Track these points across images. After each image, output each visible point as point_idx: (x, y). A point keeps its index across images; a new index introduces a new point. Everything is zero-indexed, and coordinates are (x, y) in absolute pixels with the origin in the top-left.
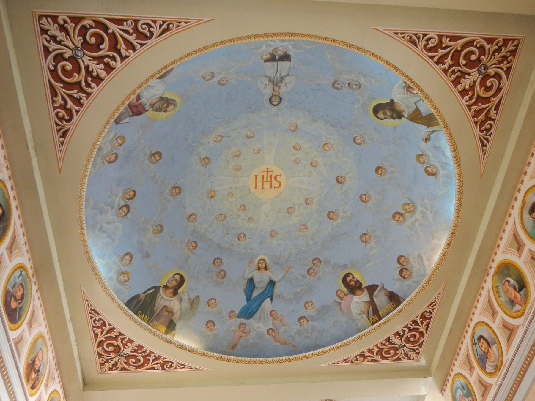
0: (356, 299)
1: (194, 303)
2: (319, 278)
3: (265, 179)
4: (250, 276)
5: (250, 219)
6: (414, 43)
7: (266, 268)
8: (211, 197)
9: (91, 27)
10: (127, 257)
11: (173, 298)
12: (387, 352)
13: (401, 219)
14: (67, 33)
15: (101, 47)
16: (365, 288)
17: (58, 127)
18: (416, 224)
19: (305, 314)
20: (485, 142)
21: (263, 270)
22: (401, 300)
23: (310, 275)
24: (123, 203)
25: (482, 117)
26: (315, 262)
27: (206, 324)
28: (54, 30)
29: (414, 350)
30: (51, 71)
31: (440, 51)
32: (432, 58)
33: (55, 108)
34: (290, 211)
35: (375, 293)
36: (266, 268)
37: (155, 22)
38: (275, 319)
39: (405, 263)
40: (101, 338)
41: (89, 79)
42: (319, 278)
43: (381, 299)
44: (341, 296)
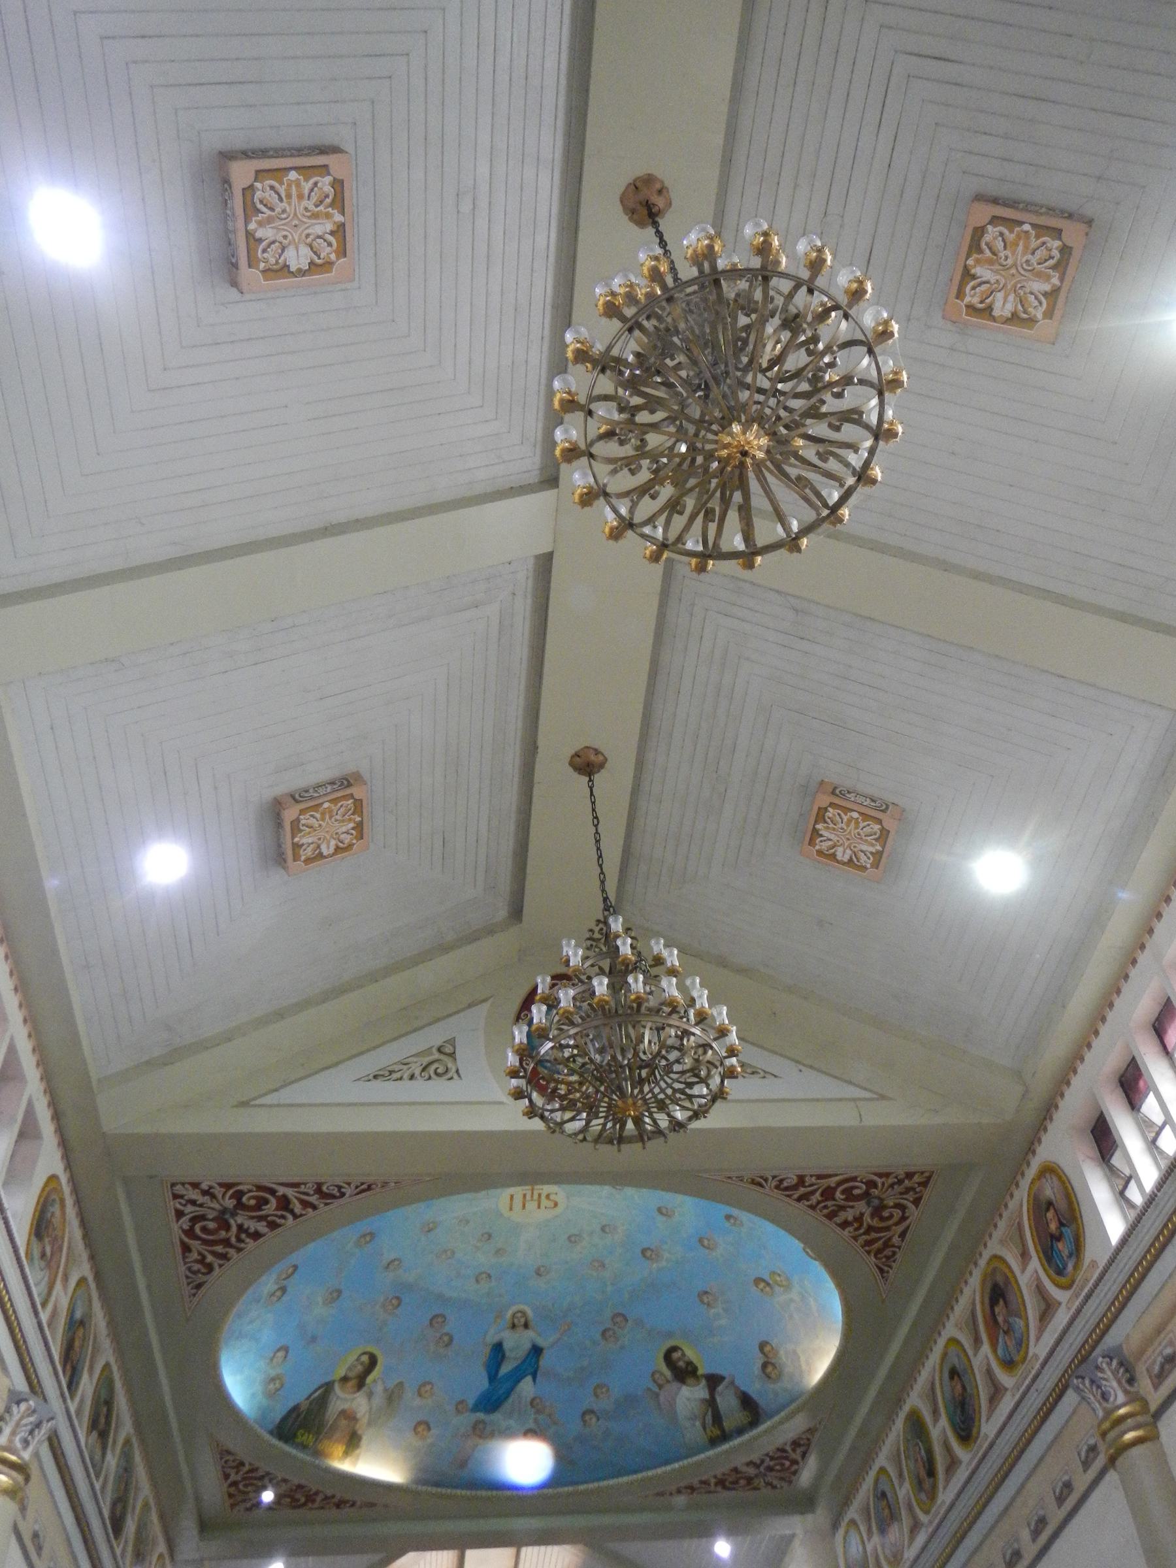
1: (393, 1397)
2: (622, 1347)
3: (528, 1197)
4: (496, 1340)
5: (499, 1252)
7: (526, 1326)
8: (430, 1231)
9: (250, 1191)
10: (281, 1354)
11: (358, 1394)
13: (768, 1289)
14: (213, 1196)
15: (264, 1207)
17: (190, 1280)
19: (595, 1407)
20: (886, 1269)
21: (520, 1330)
22: (761, 1411)
23: (606, 1340)
24: (276, 1287)
25: (879, 1244)
26: (618, 1319)
27: (415, 1428)
28: (194, 1195)
29: (782, 1479)
30: (185, 1232)
31: (803, 1189)
32: (788, 1196)
33: (185, 1263)
34: (573, 1239)
35: (720, 1388)
36: (526, 1326)
37: (349, 1184)
38: (538, 1412)
39: (771, 1355)
40: (233, 1477)
41: (243, 1236)
42: (622, 1347)
43: (727, 1401)
44: (660, 1382)
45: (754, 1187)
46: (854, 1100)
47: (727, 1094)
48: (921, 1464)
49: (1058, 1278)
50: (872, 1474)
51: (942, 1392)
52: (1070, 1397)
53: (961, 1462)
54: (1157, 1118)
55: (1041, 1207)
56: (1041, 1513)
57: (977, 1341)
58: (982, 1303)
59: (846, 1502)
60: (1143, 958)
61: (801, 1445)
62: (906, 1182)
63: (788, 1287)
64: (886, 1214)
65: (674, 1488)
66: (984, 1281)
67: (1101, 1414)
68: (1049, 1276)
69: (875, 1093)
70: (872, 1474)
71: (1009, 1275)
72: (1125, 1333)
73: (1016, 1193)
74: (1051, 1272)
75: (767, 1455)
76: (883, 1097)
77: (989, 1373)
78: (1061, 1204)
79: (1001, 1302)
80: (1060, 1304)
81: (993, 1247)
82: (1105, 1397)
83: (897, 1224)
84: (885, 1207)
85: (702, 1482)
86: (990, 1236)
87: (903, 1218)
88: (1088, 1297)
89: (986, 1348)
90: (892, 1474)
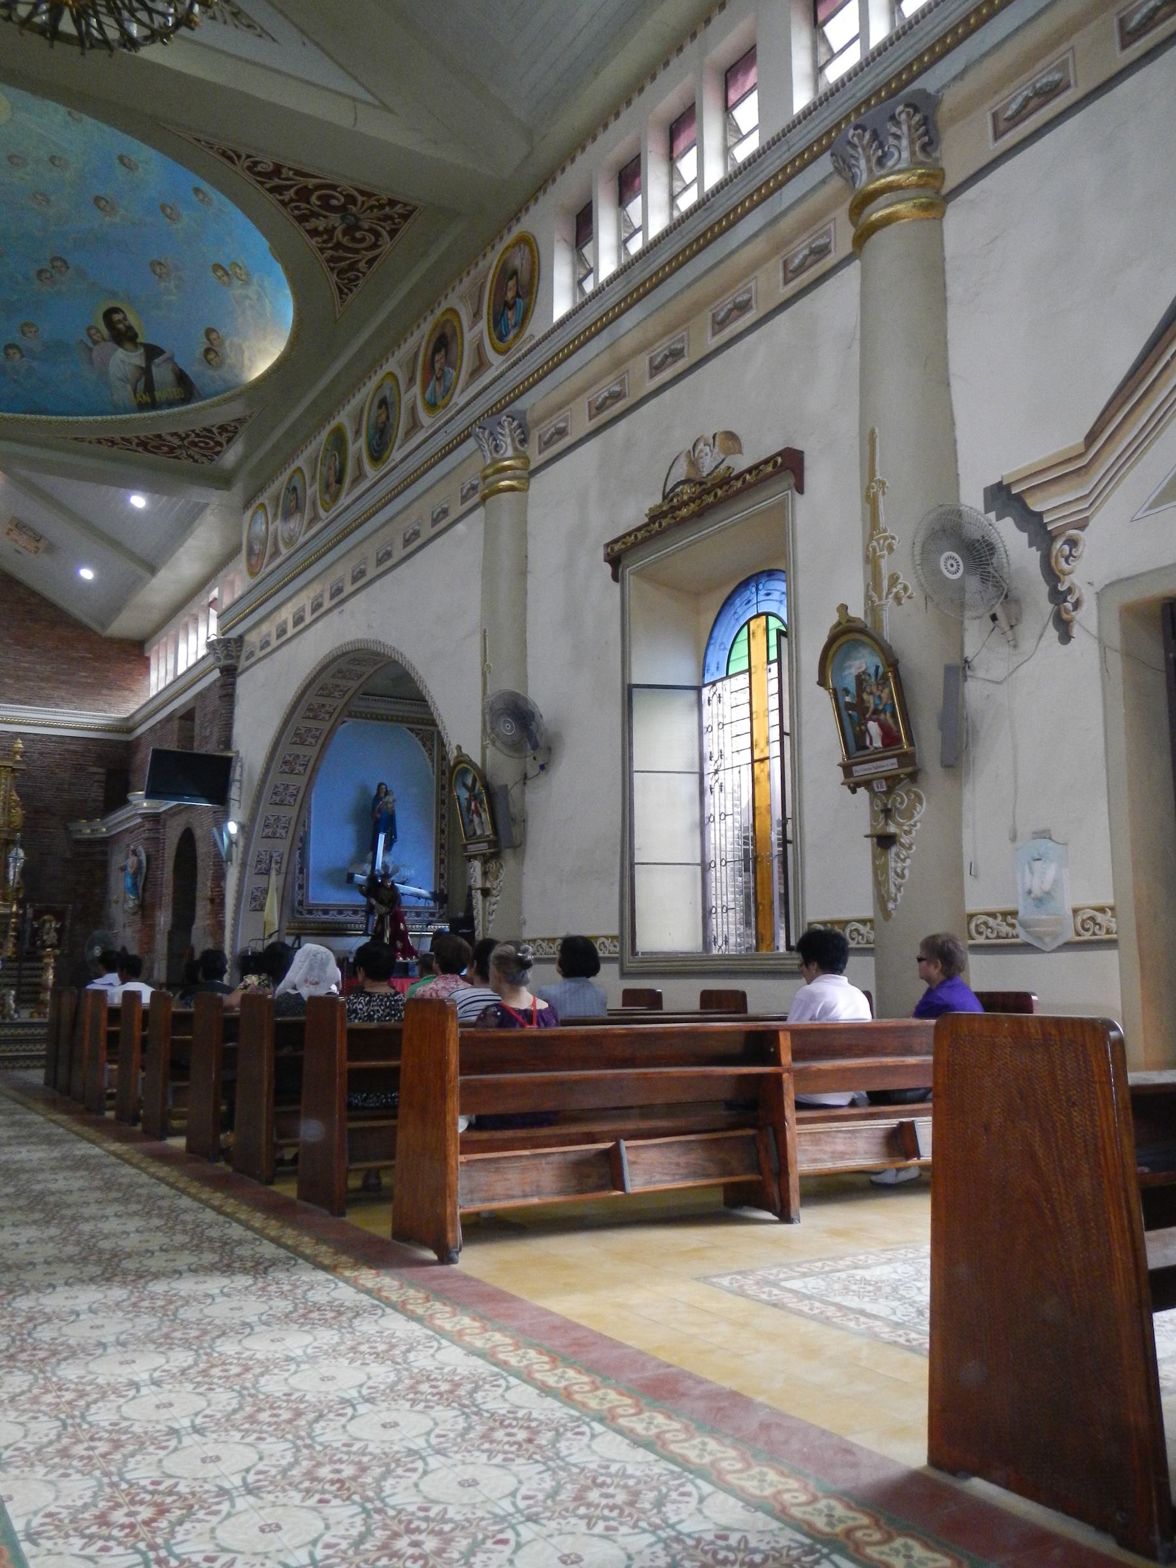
0: (120, 353)
6: (230, 159)
12: (158, 448)
13: (225, 278)
16: (142, 344)
18: (247, 302)
26: (59, 263)
32: (262, 183)
34: (15, 160)
39: (215, 343)
43: (162, 373)
45: (224, 160)
46: (354, 99)
47: (196, 24)
48: (332, 472)
49: (497, 341)
50: (289, 472)
51: (369, 417)
52: (471, 444)
53: (366, 477)
54: (637, 222)
55: (507, 273)
56: (417, 528)
57: (412, 380)
58: (426, 349)
59: (261, 489)
60: (690, 49)
61: (229, 431)
62: (387, 209)
63: (247, 283)
64: (358, 235)
65: (93, 437)
66: (434, 330)
67: (489, 462)
68: (491, 339)
69: (381, 102)
70: (289, 472)
71: (458, 329)
72: (533, 402)
73: (489, 256)
74: (494, 336)
75: (193, 431)
76: (385, 107)
77: (413, 409)
78: (524, 276)
79: (443, 352)
80: (491, 365)
81: (452, 300)
82: (497, 448)
83: (367, 249)
84: (360, 229)
85: (123, 439)
86: (453, 289)
87: (375, 246)
88: (514, 364)
89: (417, 389)
90: (305, 472)
